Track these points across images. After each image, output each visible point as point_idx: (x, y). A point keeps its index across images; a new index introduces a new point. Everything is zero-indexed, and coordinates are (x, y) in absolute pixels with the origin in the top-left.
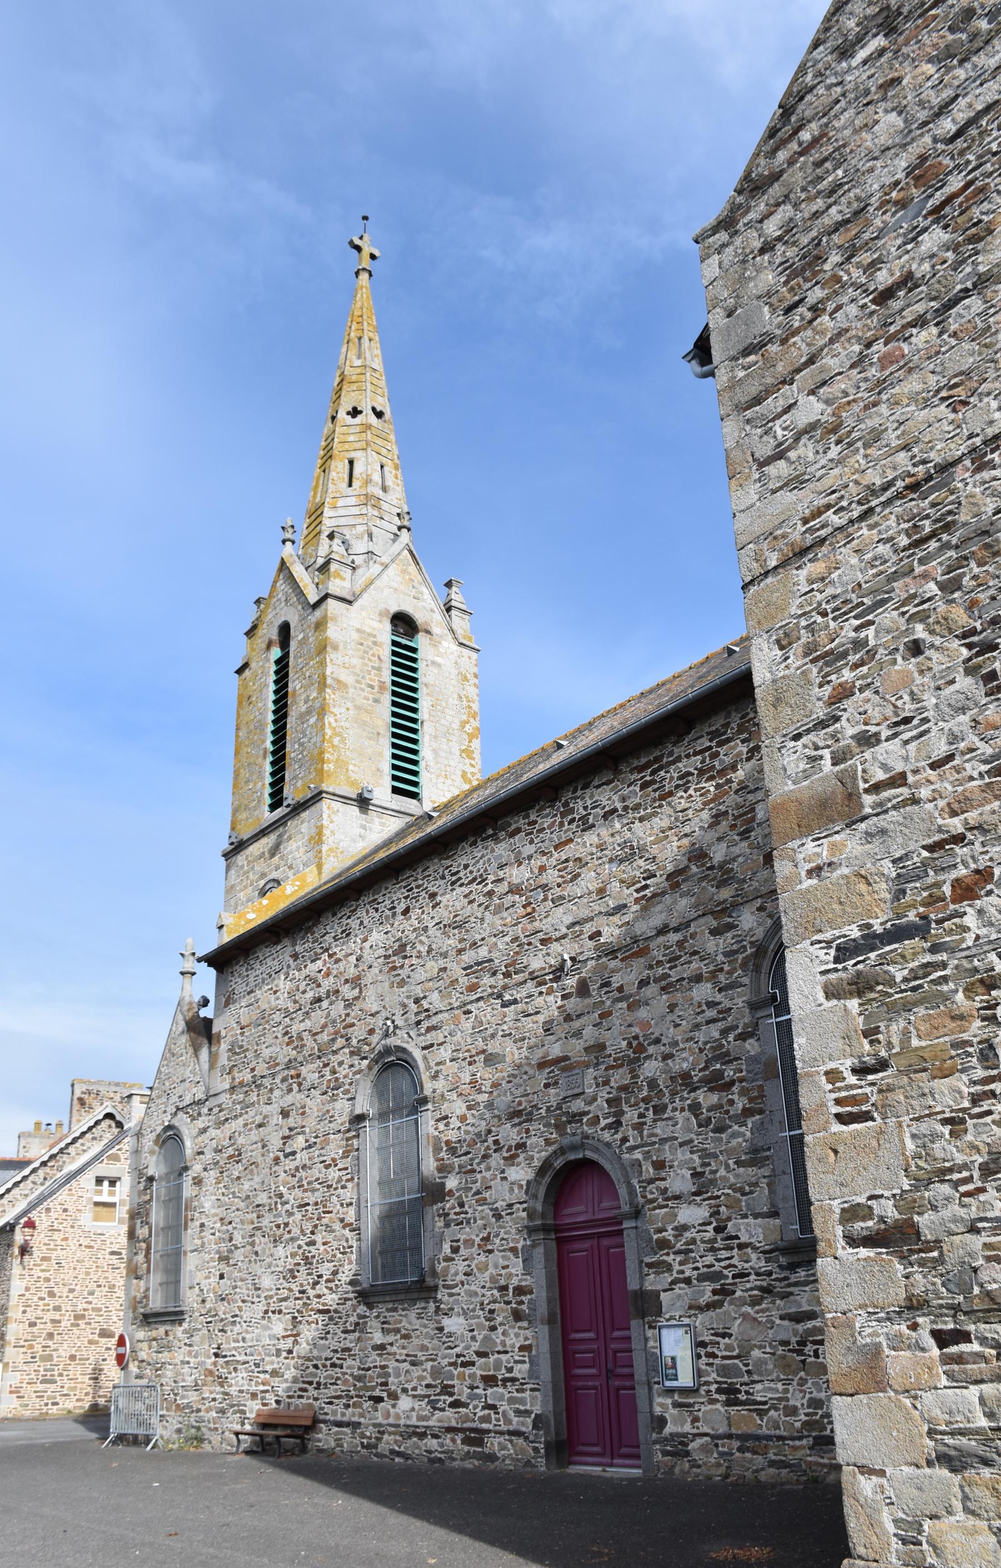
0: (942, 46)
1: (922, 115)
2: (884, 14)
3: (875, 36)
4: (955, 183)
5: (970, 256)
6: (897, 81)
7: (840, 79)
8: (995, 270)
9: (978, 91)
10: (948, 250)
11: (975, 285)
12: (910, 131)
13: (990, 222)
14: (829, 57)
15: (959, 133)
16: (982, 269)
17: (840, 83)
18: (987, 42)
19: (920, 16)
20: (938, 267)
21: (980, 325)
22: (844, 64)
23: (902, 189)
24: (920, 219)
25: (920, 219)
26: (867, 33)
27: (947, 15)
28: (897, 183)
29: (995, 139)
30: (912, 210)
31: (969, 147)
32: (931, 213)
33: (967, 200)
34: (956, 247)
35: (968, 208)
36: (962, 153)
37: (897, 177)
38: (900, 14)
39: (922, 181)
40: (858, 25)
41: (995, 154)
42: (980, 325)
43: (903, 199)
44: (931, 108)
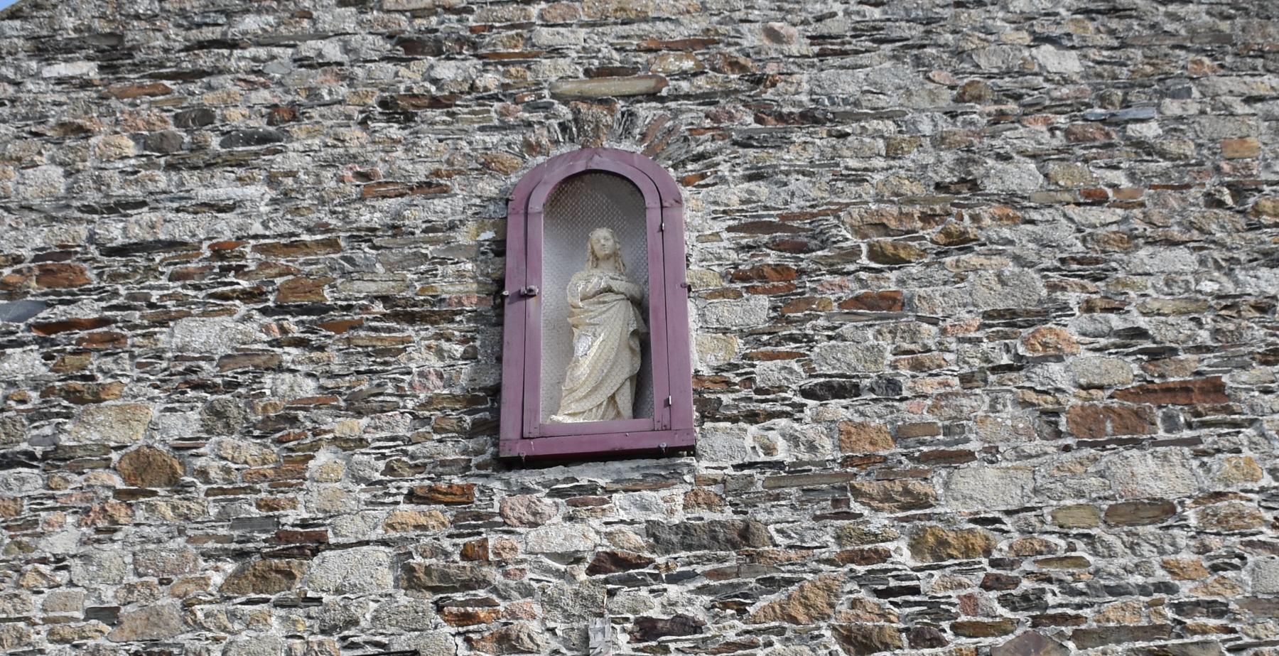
0: (159, 131)
1: (93, 197)
2: (113, 42)
3: (89, 58)
4: (88, 309)
5: (58, 415)
6: (83, 132)
7: (19, 79)
8: (80, 453)
9: (170, 215)
10: (35, 389)
11: (45, 456)
12: (68, 206)
13: (103, 386)
14: (21, 42)
15: (123, 251)
16: (64, 440)
17: (17, 84)
18: (209, 166)
19: (151, 76)
20: (12, 403)
21: (26, 513)
22: (34, 64)
23: (19, 271)
24: (22, 325)
25: (22, 325)
26: (81, 48)
27: (181, 100)
28: (17, 260)
29: (161, 288)
30: (17, 307)
31: (125, 276)
32: (38, 326)
33: (91, 340)
34: (47, 391)
35: (87, 351)
36: (115, 277)
37: (22, 252)
38: (130, 56)
39: (49, 279)
40: (76, 30)
41: (151, 306)
42: (26, 513)
43: (14, 285)
44: (107, 196)
